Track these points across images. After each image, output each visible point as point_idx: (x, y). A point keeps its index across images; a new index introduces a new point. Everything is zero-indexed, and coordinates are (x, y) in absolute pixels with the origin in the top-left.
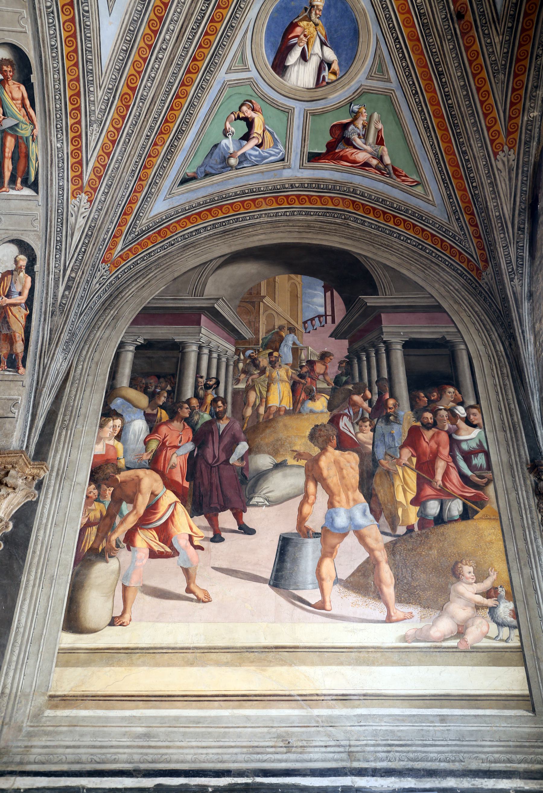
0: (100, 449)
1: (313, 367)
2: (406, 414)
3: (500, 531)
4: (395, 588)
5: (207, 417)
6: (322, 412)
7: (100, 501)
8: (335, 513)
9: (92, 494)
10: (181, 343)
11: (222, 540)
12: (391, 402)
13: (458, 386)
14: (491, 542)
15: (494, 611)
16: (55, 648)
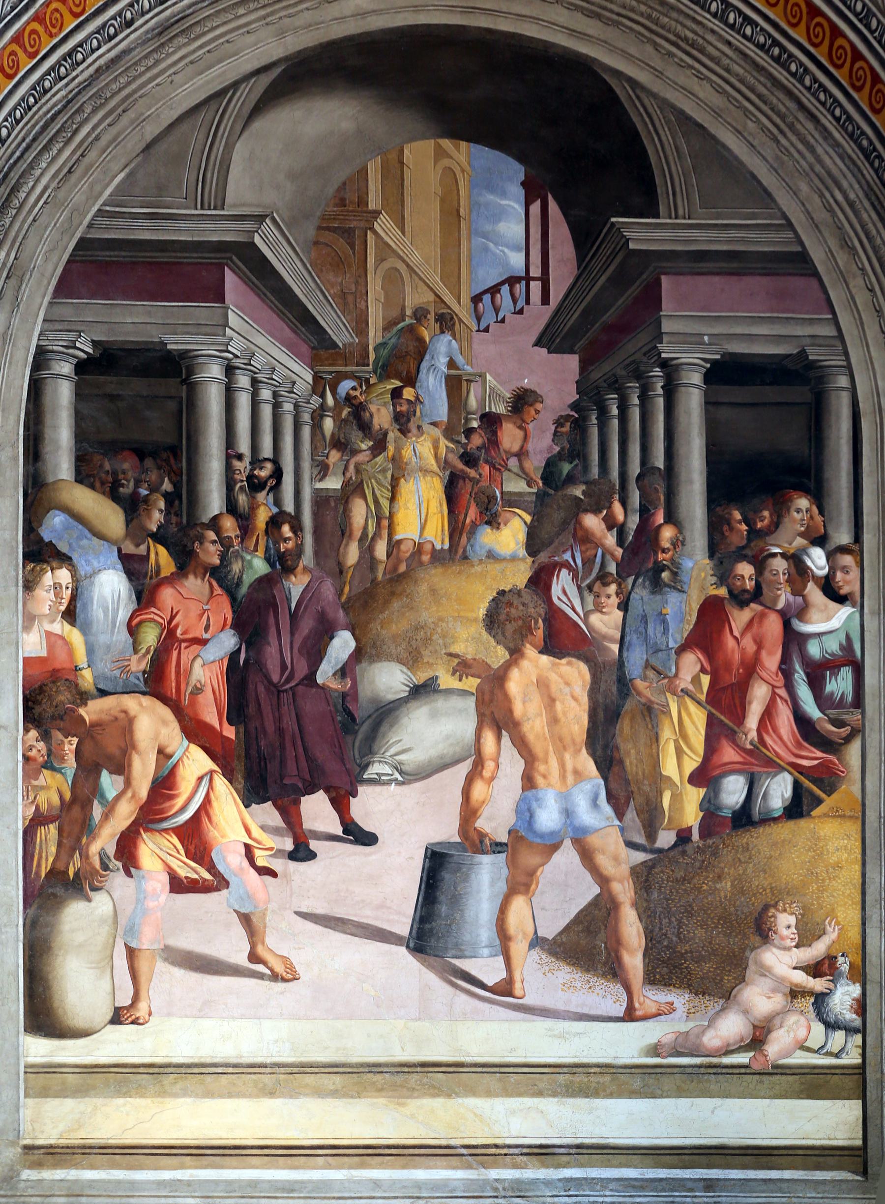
0: (33, 644)
1: (495, 433)
2: (697, 564)
3: (858, 844)
4: (644, 956)
5: (259, 566)
6: (514, 558)
7: (53, 769)
8: (537, 800)
9: (33, 753)
10: (184, 354)
11: (311, 856)
12: (667, 533)
13: (819, 496)
14: (838, 866)
15: (823, 1001)
16: (18, 1064)
